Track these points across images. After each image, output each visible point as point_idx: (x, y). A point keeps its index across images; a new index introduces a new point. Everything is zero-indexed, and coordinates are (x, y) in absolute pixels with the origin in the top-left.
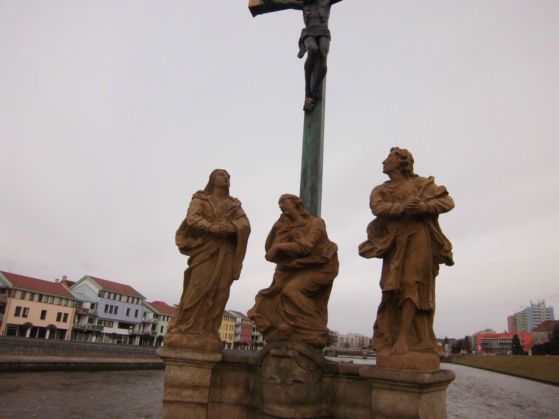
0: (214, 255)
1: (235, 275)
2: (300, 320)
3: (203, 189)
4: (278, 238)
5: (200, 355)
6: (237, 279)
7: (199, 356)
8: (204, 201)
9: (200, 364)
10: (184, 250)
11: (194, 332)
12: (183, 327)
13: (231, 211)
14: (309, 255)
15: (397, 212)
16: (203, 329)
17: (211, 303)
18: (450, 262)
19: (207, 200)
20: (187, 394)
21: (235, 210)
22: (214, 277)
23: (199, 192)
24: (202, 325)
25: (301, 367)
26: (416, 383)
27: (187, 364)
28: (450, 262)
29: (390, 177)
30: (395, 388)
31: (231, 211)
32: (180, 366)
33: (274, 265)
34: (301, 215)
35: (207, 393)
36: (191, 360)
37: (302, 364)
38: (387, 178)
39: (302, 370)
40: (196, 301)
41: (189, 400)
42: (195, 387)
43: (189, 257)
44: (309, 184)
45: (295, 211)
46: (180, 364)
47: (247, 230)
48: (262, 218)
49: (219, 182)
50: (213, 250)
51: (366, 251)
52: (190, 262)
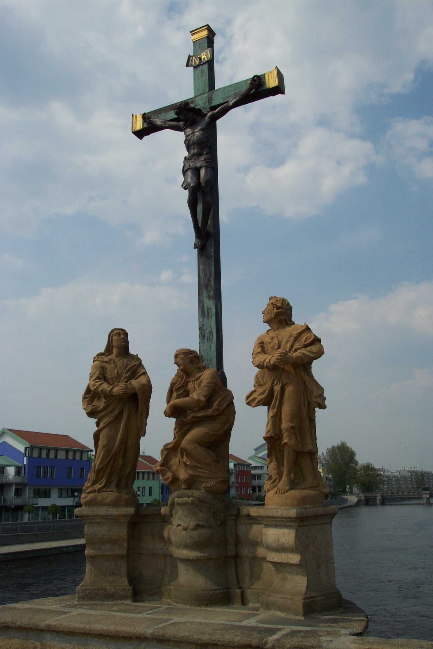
1: (141, 432)
3: (102, 350)
4: (175, 394)
6: (144, 435)
7: (113, 511)
8: (104, 364)
10: (91, 414)
12: (98, 486)
13: (132, 370)
16: (117, 486)
18: (323, 407)
19: (106, 362)
21: (136, 368)
23: (100, 354)
24: (115, 483)
25: (203, 512)
26: (289, 518)
27: (104, 521)
28: (323, 407)
29: (270, 326)
31: (132, 370)
32: (99, 523)
33: (173, 420)
36: (107, 516)
37: (204, 510)
38: (267, 327)
40: (107, 461)
42: (114, 542)
43: (96, 420)
46: (97, 520)
47: (148, 388)
48: (161, 375)
49: (119, 342)
50: (117, 412)
51: (250, 401)
52: (98, 424)
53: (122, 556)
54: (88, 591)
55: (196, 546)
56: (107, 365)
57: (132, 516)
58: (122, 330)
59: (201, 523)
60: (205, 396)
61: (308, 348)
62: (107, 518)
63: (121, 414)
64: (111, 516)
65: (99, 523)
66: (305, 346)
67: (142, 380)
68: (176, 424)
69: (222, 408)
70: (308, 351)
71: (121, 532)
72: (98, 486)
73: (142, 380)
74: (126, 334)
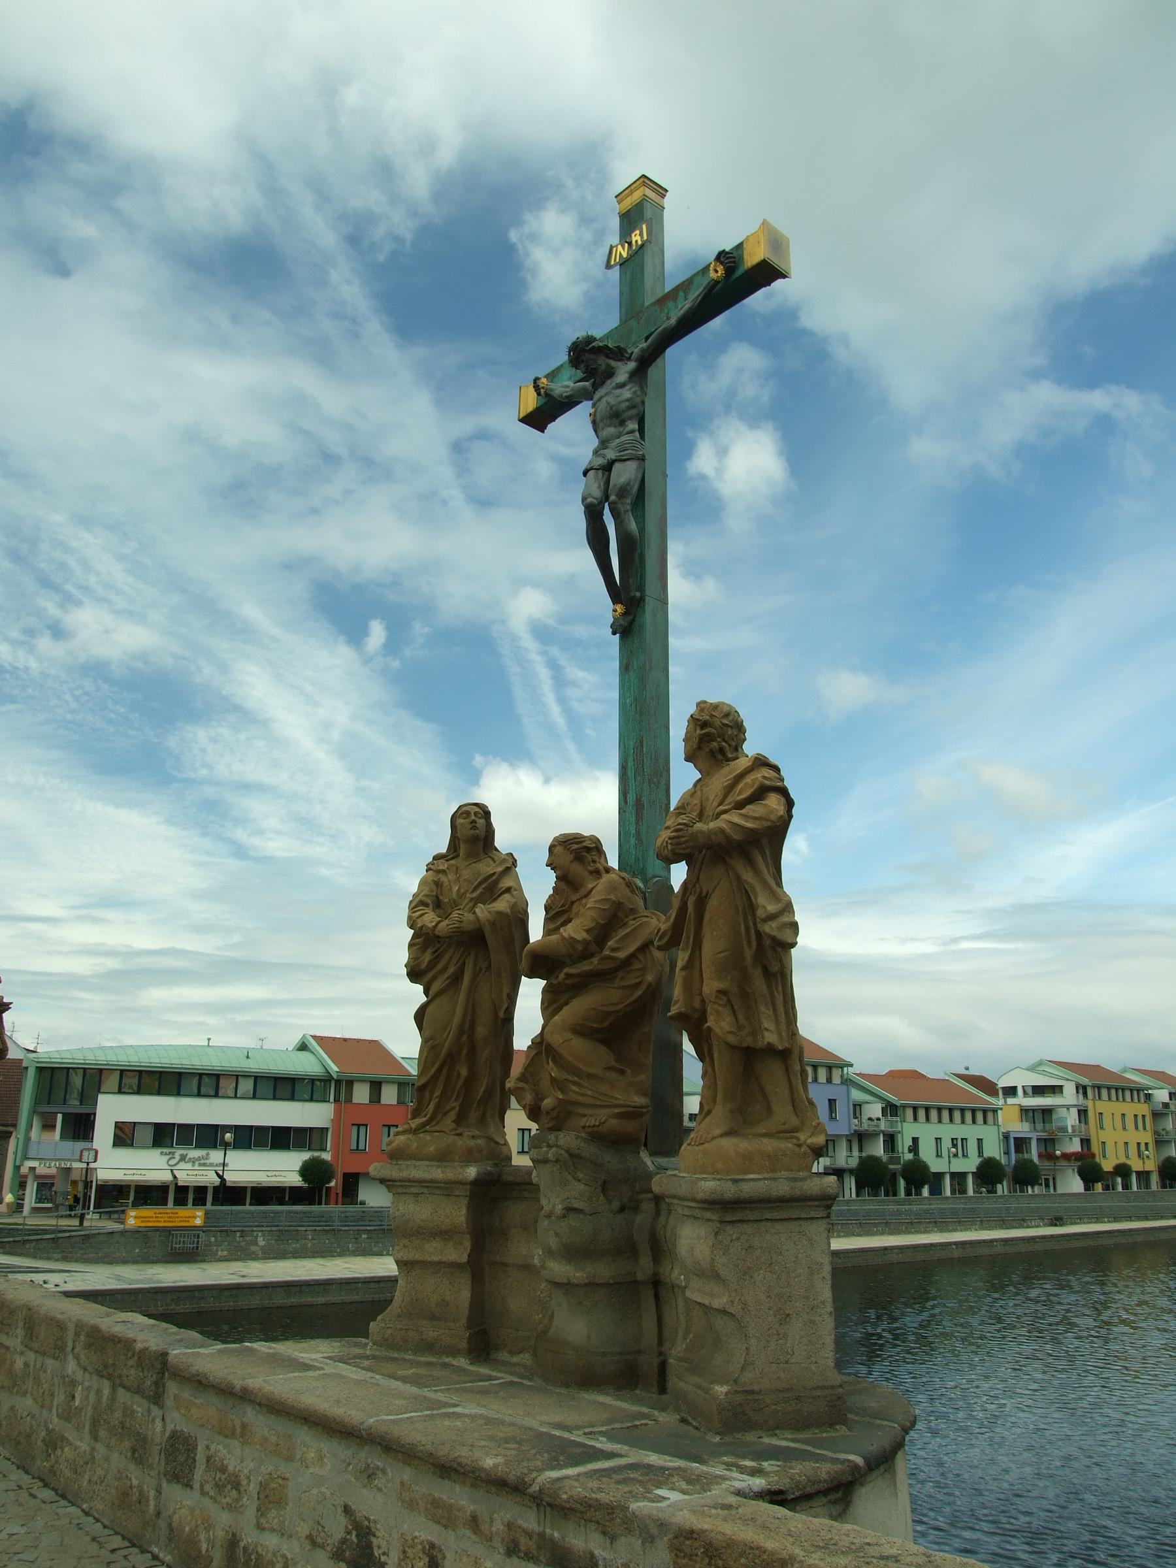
0: (457, 979)
2: (574, 1088)
5: (439, 1170)
7: (438, 1173)
9: (446, 1188)
11: (437, 1128)
14: (586, 955)
17: (464, 1072)
19: (443, 871)
20: (434, 1251)
22: (456, 1021)
24: (453, 1115)
27: (425, 1190)
32: (416, 1195)
34: (591, 872)
35: (468, 1244)
37: (580, 1175)
39: (582, 1187)
40: (433, 1070)
41: (435, 1259)
42: (446, 1234)
44: (631, 798)
45: (576, 868)
46: (413, 1190)
50: (451, 970)
53: (455, 1266)
54: (389, 1331)
55: (574, 1253)
56: (443, 879)
57: (476, 1183)
58: (476, 805)
59: (576, 1206)
60: (588, 931)
61: (749, 809)
62: (429, 1185)
64: (432, 1181)
65: (416, 1195)
66: (740, 805)
67: (502, 905)
68: (545, 991)
69: (622, 955)
70: (745, 816)
71: (457, 1213)
72: (414, 1124)
73: (502, 905)
74: (487, 814)
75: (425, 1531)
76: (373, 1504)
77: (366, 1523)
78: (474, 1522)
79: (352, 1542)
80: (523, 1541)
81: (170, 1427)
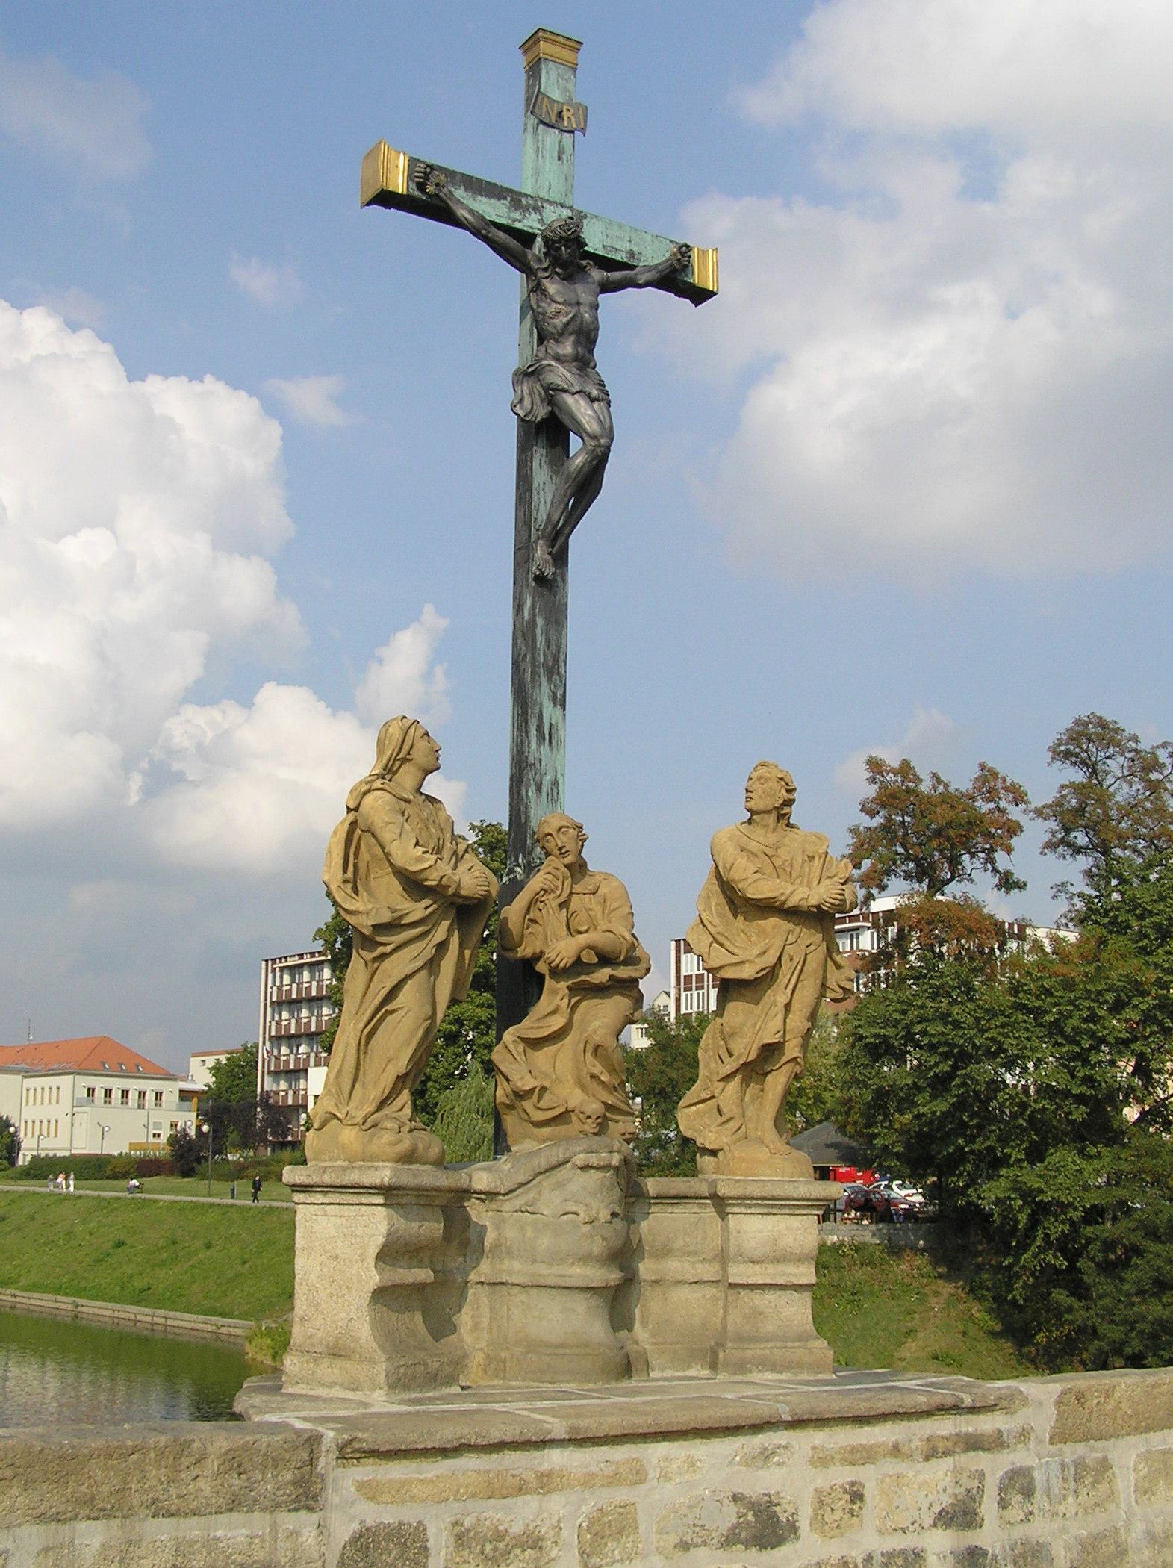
15: (803, 903)
30: (774, 1211)
54: (402, 1370)
63: (442, 947)
75: (842, 1475)
76: (762, 1482)
77: (766, 1498)
78: (896, 1450)
79: (748, 1523)
80: (941, 1446)
81: (343, 1530)
